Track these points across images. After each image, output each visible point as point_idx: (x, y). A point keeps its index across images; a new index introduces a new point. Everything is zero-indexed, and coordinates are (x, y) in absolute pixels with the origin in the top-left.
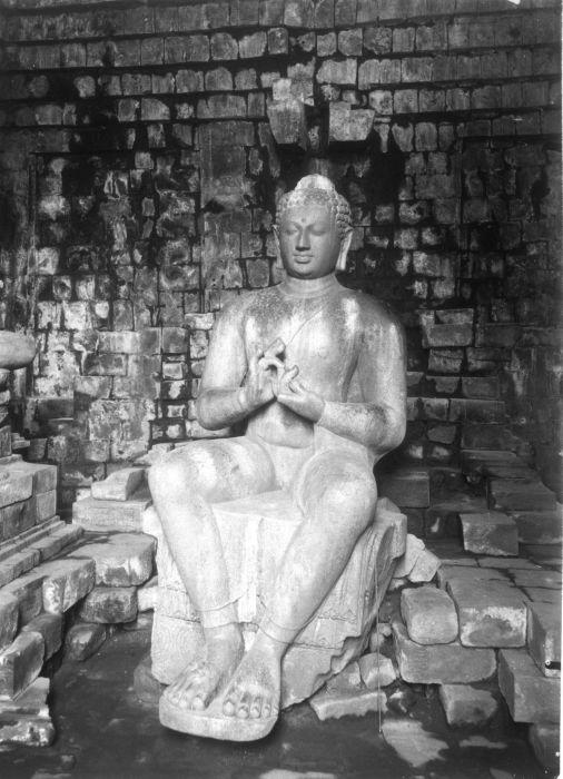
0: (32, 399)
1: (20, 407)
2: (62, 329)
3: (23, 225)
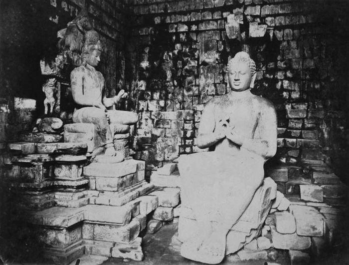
0: (136, 137)
2: (147, 110)
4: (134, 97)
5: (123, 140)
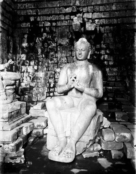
0: (20, 87)
1: (17, 89)
2: (27, 72)
3: (18, 49)
5: (11, 90)
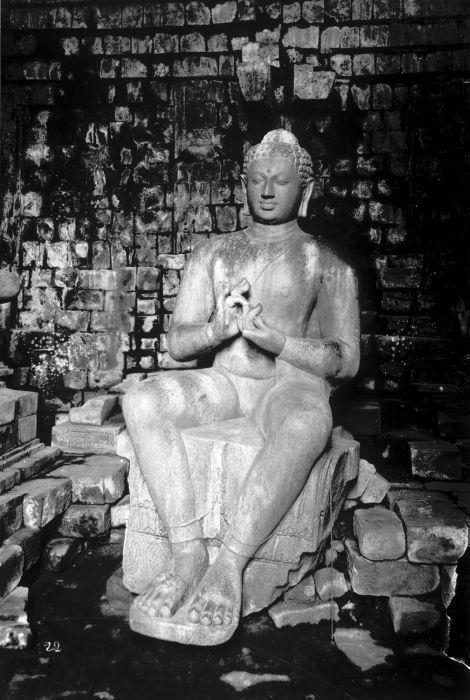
0: (16, 331)
2: (45, 266)
4: (9, 233)
